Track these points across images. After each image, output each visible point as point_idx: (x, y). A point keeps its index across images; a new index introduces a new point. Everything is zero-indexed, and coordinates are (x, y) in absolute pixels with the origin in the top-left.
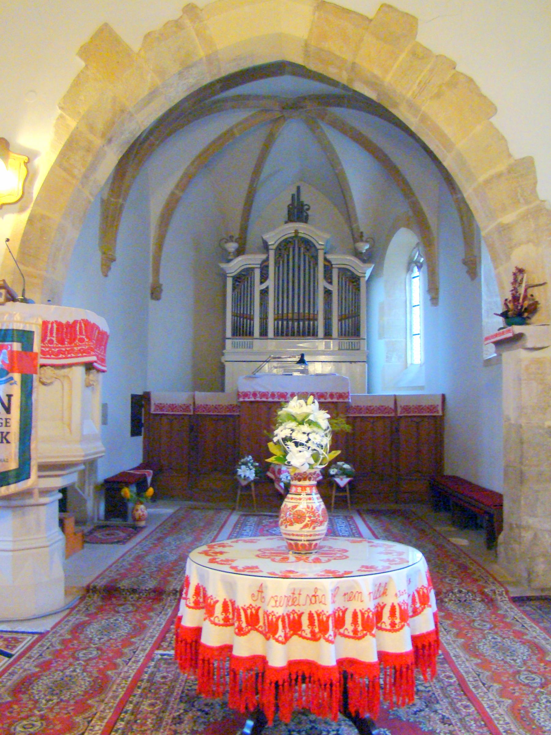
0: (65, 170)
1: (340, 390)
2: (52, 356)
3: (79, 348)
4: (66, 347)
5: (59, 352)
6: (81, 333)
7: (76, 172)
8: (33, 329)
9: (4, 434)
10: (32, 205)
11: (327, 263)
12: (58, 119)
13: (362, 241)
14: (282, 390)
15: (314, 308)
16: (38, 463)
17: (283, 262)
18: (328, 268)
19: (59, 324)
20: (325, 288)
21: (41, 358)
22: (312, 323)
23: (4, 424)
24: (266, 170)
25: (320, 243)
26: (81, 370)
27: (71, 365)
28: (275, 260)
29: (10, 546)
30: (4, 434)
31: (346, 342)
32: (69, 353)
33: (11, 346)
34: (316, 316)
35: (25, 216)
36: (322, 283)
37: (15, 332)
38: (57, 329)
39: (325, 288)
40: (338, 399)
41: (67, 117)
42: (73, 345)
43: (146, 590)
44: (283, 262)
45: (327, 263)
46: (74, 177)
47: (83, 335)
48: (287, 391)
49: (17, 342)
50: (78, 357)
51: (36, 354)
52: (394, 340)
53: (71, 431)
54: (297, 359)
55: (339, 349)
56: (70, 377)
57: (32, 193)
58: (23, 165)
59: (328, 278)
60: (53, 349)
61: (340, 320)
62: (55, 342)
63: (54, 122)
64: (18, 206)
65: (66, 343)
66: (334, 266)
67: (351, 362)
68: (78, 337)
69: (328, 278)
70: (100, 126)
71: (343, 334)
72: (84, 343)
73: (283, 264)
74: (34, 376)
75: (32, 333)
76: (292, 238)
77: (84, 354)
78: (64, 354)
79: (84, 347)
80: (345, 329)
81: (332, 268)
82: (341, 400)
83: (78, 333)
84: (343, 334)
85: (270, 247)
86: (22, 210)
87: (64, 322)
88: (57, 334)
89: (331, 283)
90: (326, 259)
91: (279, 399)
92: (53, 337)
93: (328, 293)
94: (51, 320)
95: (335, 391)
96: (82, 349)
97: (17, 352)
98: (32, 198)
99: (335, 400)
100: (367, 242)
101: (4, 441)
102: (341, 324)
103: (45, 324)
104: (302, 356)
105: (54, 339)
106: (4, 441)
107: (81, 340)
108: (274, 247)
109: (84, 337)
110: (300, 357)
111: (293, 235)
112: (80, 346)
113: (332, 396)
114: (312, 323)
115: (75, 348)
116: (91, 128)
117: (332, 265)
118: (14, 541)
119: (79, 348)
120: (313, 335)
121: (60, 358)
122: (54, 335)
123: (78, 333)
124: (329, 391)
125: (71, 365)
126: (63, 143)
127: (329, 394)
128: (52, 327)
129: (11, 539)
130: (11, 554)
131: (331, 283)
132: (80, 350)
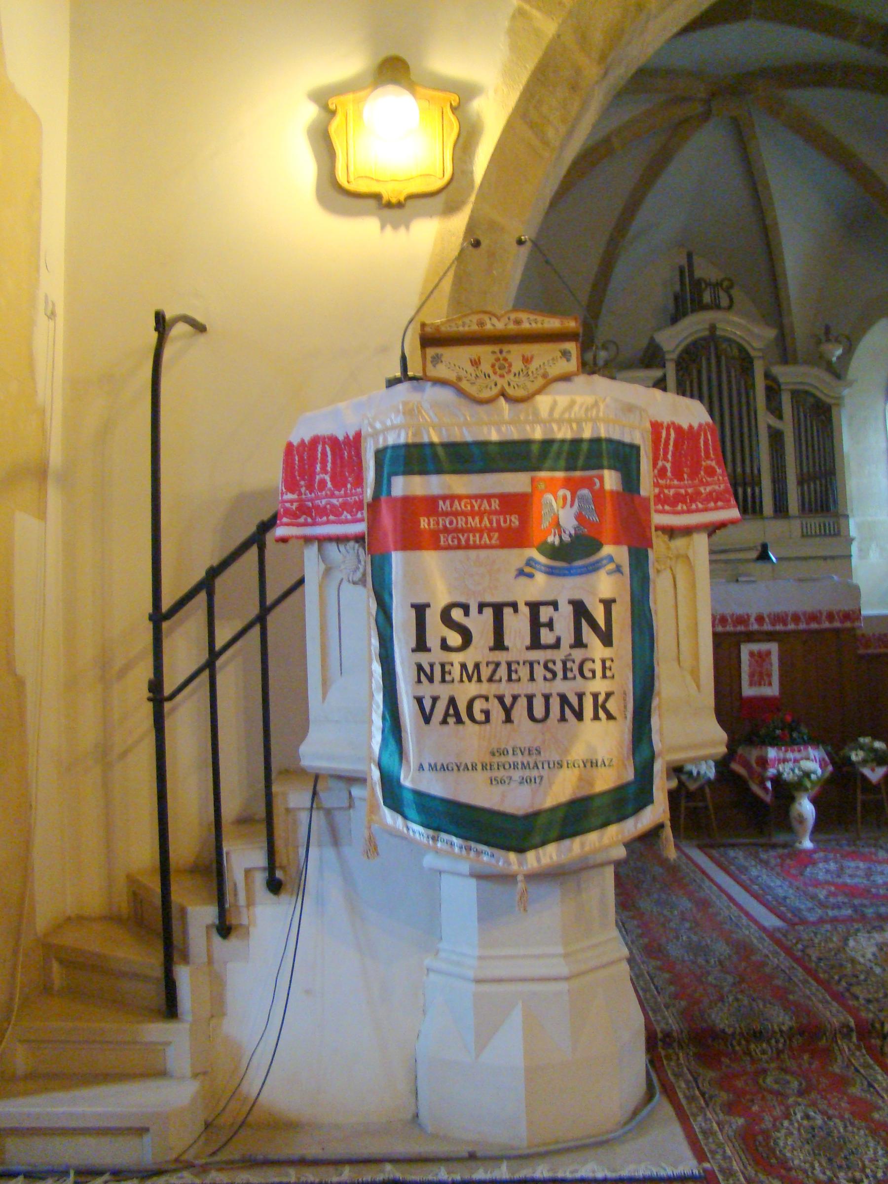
0: (531, 125)
1: (846, 607)
2: (667, 508)
3: (708, 489)
4: (685, 487)
5: (678, 499)
6: (708, 457)
7: (550, 133)
8: (637, 440)
9: (601, 699)
10: (473, 198)
11: (770, 383)
12: (514, 17)
13: (828, 340)
14: (740, 611)
15: (752, 461)
16: (668, 763)
17: (691, 382)
18: (773, 391)
19: (679, 429)
20: (769, 427)
21: (657, 511)
22: (749, 490)
23: (599, 673)
24: (638, 223)
25: (755, 345)
26: (701, 541)
27: (688, 531)
28: (678, 379)
29: (565, 971)
30: (601, 699)
31: (814, 522)
32: (693, 500)
33: (601, 478)
34: (756, 479)
35: (459, 222)
36: (765, 419)
37: (604, 446)
38: (676, 441)
39: (769, 427)
40: (842, 622)
41: (535, 13)
42: (696, 482)
43: (781, 1031)
44: (691, 382)
45: (770, 383)
46: (546, 143)
47: (712, 460)
48: (750, 612)
49: (610, 468)
50: (711, 509)
51: (647, 500)
52: (869, 519)
53: (698, 687)
54: (754, 555)
55: (803, 536)
56: (692, 559)
57: (472, 173)
58: (448, 110)
59: (776, 410)
60: (666, 491)
61: (800, 483)
62: (669, 474)
63: (507, 24)
64: (442, 198)
65: (686, 476)
66: (783, 387)
67: (825, 558)
68: (704, 463)
69: (776, 410)
70: (597, 38)
71: (806, 509)
72: (716, 478)
73: (691, 387)
74: (649, 550)
75: (635, 449)
76: (704, 339)
77: (720, 504)
78: (684, 502)
79: (716, 487)
80: (810, 499)
81: (780, 390)
82: (848, 624)
83: (703, 454)
84: (806, 509)
85: (668, 357)
86: (451, 209)
87: (685, 426)
88: (673, 455)
89: (780, 417)
90: (767, 376)
91: (774, 625)
92: (668, 461)
93: (776, 437)
94: (665, 418)
95: (835, 608)
96: (715, 491)
97: (612, 492)
98: (472, 181)
99: (837, 624)
100: (837, 340)
101: (601, 714)
102: (802, 490)
103: (656, 427)
104: (765, 547)
105: (668, 466)
106: (601, 714)
107: (711, 472)
108: (674, 356)
109: (713, 464)
110: (759, 548)
111: (707, 333)
112: (708, 484)
113: (830, 617)
114: (749, 490)
115: (702, 489)
116: (583, 39)
117: (779, 385)
118: (566, 956)
119: (708, 489)
120: (754, 512)
121: (679, 513)
122: (670, 457)
123: (703, 454)
124: (825, 608)
125: (688, 531)
126: (530, 66)
127: (825, 614)
128: (668, 434)
129: (560, 950)
130: (563, 986)
131: (780, 417)
132: (710, 493)
